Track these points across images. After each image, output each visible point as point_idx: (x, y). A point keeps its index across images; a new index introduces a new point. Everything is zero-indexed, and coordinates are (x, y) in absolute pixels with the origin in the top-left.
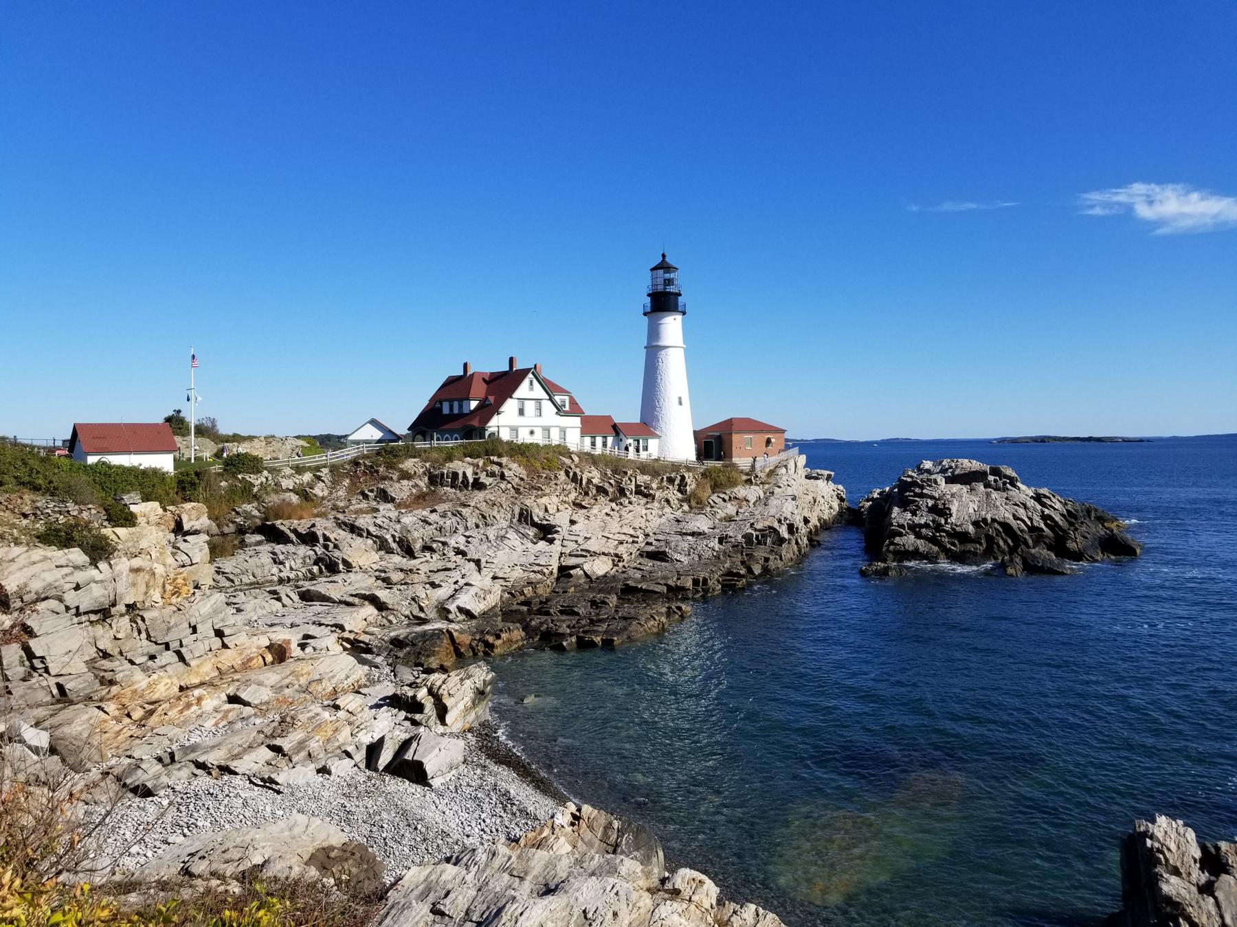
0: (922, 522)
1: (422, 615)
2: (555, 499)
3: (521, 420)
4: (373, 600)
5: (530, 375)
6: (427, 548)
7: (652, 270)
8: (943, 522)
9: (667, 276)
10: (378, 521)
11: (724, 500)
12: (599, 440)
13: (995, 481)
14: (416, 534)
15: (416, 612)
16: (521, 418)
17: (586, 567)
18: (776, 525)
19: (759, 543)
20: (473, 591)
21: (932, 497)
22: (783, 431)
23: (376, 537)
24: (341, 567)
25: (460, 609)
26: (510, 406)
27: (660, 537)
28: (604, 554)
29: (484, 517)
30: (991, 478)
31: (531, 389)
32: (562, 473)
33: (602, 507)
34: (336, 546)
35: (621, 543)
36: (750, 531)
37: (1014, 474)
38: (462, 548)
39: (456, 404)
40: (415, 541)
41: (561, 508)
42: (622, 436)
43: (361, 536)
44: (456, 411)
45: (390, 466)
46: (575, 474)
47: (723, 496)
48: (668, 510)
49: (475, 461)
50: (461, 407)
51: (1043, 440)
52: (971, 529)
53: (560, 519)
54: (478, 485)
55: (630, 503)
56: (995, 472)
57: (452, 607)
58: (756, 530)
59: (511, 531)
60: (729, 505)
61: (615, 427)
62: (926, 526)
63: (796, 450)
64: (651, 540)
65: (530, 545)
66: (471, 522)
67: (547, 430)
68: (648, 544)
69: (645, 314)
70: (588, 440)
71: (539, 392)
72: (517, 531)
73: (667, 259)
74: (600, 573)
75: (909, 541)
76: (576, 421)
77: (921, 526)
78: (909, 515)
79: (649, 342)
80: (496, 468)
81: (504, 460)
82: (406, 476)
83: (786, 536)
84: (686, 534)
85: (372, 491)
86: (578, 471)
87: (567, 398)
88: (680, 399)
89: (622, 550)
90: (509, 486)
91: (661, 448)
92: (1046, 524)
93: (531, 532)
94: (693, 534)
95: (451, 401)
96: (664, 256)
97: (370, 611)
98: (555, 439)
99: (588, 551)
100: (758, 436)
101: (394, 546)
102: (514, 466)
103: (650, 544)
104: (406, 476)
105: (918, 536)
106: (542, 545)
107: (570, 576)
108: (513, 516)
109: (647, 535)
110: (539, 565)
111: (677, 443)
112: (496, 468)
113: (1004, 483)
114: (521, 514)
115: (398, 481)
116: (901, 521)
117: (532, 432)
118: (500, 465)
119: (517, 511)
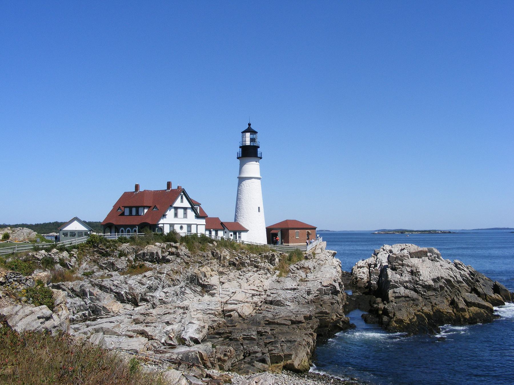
0: (407, 279)
3: (177, 220)
6: (144, 300)
7: (243, 132)
8: (418, 279)
9: (252, 136)
10: (115, 283)
11: (298, 269)
12: (213, 233)
13: (431, 256)
14: (137, 291)
16: (176, 219)
18: (334, 284)
19: (325, 294)
21: (408, 266)
22: (315, 228)
24: (102, 312)
25: (191, 338)
26: (170, 213)
28: (247, 302)
31: (182, 201)
32: (210, 253)
33: (233, 273)
34: (98, 299)
35: (253, 295)
36: (320, 287)
37: (439, 253)
39: (134, 211)
42: (226, 230)
44: (134, 213)
46: (217, 253)
47: (297, 266)
48: (269, 275)
50: (137, 212)
52: (432, 283)
53: (214, 280)
54: (165, 261)
56: (431, 251)
57: (186, 336)
59: (187, 289)
60: (300, 271)
61: (222, 223)
64: (268, 293)
65: (200, 297)
67: (189, 226)
68: (267, 295)
69: (238, 158)
72: (191, 288)
75: (401, 290)
77: (406, 282)
78: (399, 276)
81: (178, 244)
83: (338, 288)
86: (218, 251)
88: (259, 208)
89: (256, 299)
90: (182, 260)
92: (463, 279)
93: (199, 289)
94: (291, 289)
95: (131, 208)
96: (249, 125)
97: (144, 340)
98: (194, 231)
99: (236, 300)
102: (183, 248)
103: (270, 296)
105: (406, 288)
106: (207, 297)
107: (230, 316)
108: (187, 279)
110: (212, 310)
111: (256, 235)
112: (174, 250)
116: (396, 280)
117: (181, 228)
118: (176, 248)
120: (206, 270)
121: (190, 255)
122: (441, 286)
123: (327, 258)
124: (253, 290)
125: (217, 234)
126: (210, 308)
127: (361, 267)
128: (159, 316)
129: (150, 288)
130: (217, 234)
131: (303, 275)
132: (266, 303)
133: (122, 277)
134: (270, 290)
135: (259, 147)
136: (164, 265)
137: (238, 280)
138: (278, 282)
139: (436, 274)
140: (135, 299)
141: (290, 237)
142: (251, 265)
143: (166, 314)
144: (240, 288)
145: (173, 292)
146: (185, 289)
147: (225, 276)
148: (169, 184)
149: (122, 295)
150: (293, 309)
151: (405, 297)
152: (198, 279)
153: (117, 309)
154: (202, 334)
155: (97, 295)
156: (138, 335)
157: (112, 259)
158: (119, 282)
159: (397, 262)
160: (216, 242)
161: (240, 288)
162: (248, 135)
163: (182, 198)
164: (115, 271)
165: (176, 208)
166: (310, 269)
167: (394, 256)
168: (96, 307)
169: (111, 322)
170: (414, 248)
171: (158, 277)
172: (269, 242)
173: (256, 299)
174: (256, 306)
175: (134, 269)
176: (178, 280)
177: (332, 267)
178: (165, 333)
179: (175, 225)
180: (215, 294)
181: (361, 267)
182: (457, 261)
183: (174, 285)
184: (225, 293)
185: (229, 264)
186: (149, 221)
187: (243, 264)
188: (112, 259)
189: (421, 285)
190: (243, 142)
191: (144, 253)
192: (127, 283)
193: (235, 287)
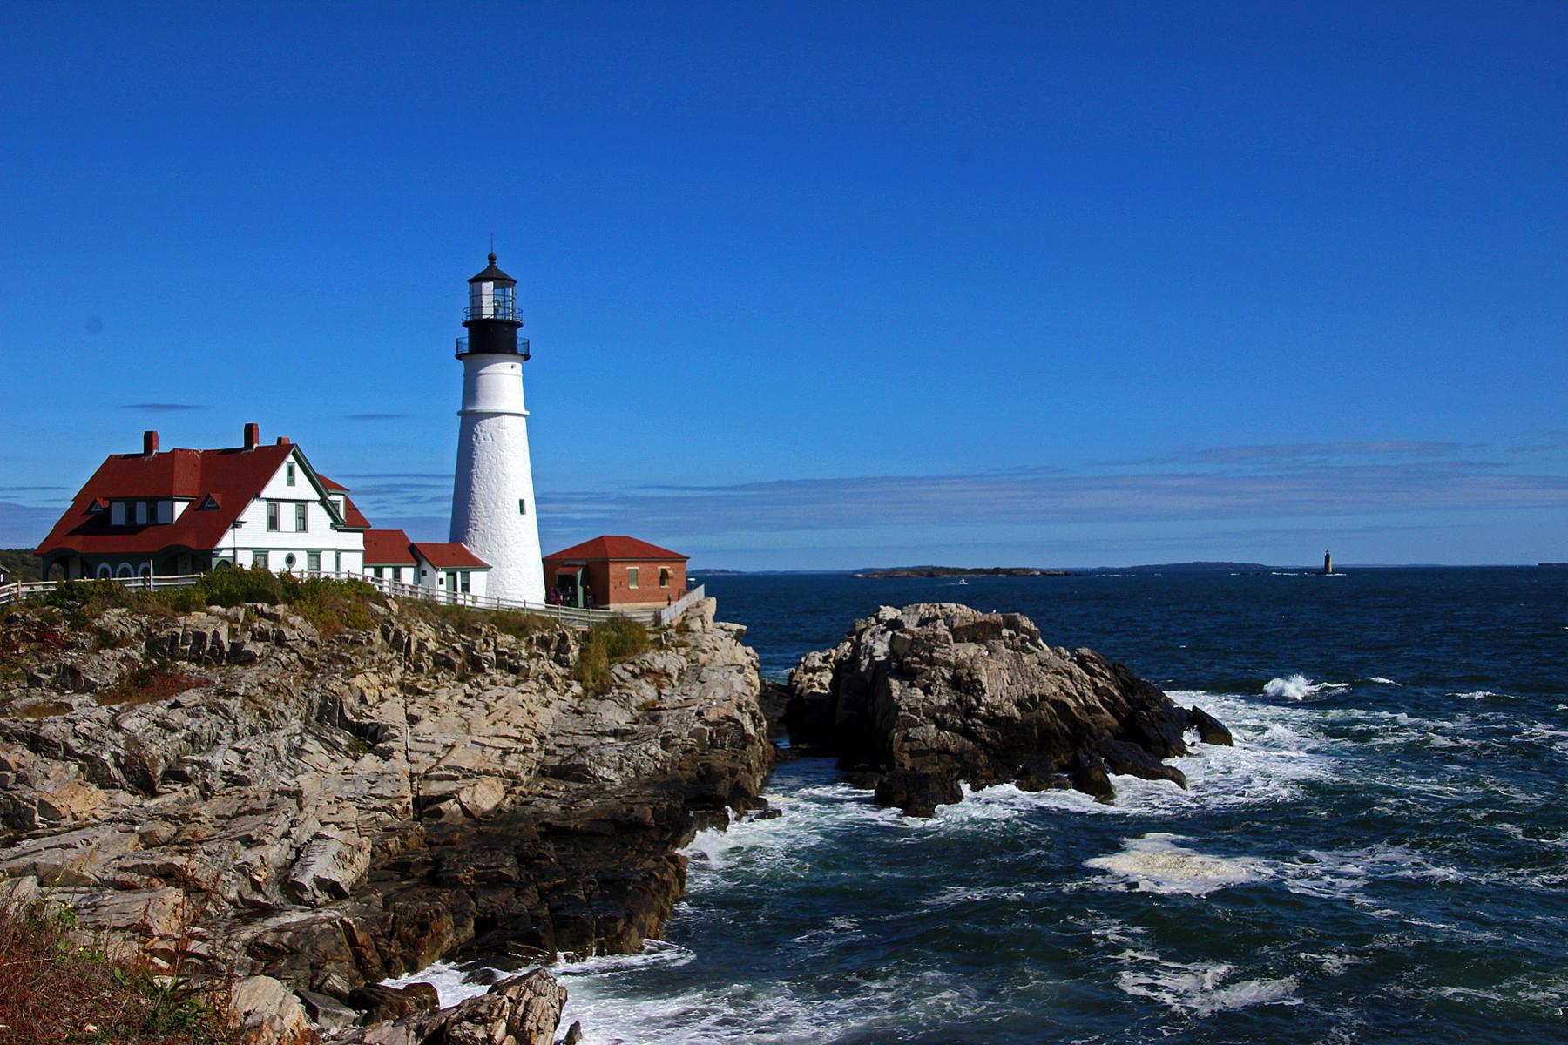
0: (944, 702)
1: (260, 898)
2: (374, 679)
4: (169, 875)
5: (291, 458)
6: (175, 774)
7: (471, 281)
9: (499, 291)
10: (82, 727)
11: (634, 675)
12: (388, 573)
13: (1011, 637)
15: (249, 894)
16: (274, 534)
17: (464, 797)
18: (737, 714)
20: (333, 848)
21: (947, 664)
23: (83, 757)
24: (37, 817)
25: (321, 883)
26: (255, 513)
27: (562, 741)
28: (486, 772)
29: (264, 714)
30: (1005, 632)
31: (291, 482)
32: (377, 632)
33: (448, 692)
34: (22, 779)
36: (698, 725)
38: (238, 772)
40: (154, 761)
41: (387, 693)
42: (426, 567)
43: (56, 758)
44: (141, 518)
45: (79, 623)
46: (398, 633)
47: (631, 668)
48: (551, 693)
49: (232, 611)
50: (152, 513)
51: (997, 571)
53: (391, 712)
54: (241, 657)
55: (493, 682)
56: (1012, 624)
57: (307, 880)
58: (707, 723)
59: (309, 738)
60: (643, 682)
62: (950, 708)
63: (702, 588)
65: (349, 762)
66: (245, 721)
67: (315, 554)
68: (548, 752)
69: (459, 357)
70: (370, 572)
71: (304, 488)
73: (498, 264)
74: (487, 806)
76: (356, 540)
77: (944, 710)
79: (464, 405)
80: (266, 625)
81: (281, 609)
82: (106, 640)
84: (603, 734)
85: (48, 671)
86: (402, 627)
87: (341, 498)
88: (522, 502)
89: (513, 762)
90: (294, 656)
91: (490, 585)
92: (1102, 702)
93: (343, 738)
94: (615, 733)
96: (492, 259)
100: (646, 567)
101: (116, 773)
104: (106, 640)
105: (941, 725)
106: (369, 762)
107: (440, 813)
108: (310, 709)
109: (541, 738)
110: (382, 797)
112: (266, 625)
113: (1023, 641)
114: (323, 707)
115: (95, 651)
116: (913, 703)
117: (290, 560)
119: (316, 698)
120: (366, 683)
121: (317, 639)
122: (1040, 721)
123: (719, 644)
124: (506, 737)
125: (397, 576)
126: (378, 791)
127: (814, 670)
128: (220, 822)
129: (193, 739)
130: (397, 576)
131: (649, 692)
132: (543, 773)
133: (104, 713)
134: (553, 735)
135: (520, 325)
136: (238, 669)
137: (461, 709)
138: (579, 713)
139: (1024, 688)
140: (145, 773)
141: (611, 587)
142: (500, 664)
143: (244, 813)
144: (468, 732)
145: (264, 750)
146: (303, 741)
147: (421, 700)
148: (250, 431)
149: (104, 763)
150: (620, 790)
151: (939, 752)
152: (341, 709)
153: (88, 808)
154: (353, 868)
155: (19, 766)
156: (155, 881)
157: (71, 658)
158: (94, 725)
159: (916, 655)
160: (396, 599)
161: (468, 732)
162: (488, 287)
163: (291, 472)
164: (83, 691)
165: (274, 502)
166: (669, 676)
167: (908, 637)
168: (16, 804)
169: (63, 847)
170: (963, 613)
171: (219, 705)
172: (549, 600)
173: (513, 762)
174: (514, 784)
175: (143, 684)
176: (281, 714)
177: (733, 669)
178: (241, 870)
179: (271, 554)
180: (392, 750)
181: (814, 670)
182: (1085, 651)
183: (269, 729)
184: (420, 746)
185: (435, 664)
186: (190, 541)
187: (476, 665)
188: (71, 658)
189: (983, 718)
190: (473, 308)
191: (175, 637)
192: (118, 729)
193: (453, 730)
